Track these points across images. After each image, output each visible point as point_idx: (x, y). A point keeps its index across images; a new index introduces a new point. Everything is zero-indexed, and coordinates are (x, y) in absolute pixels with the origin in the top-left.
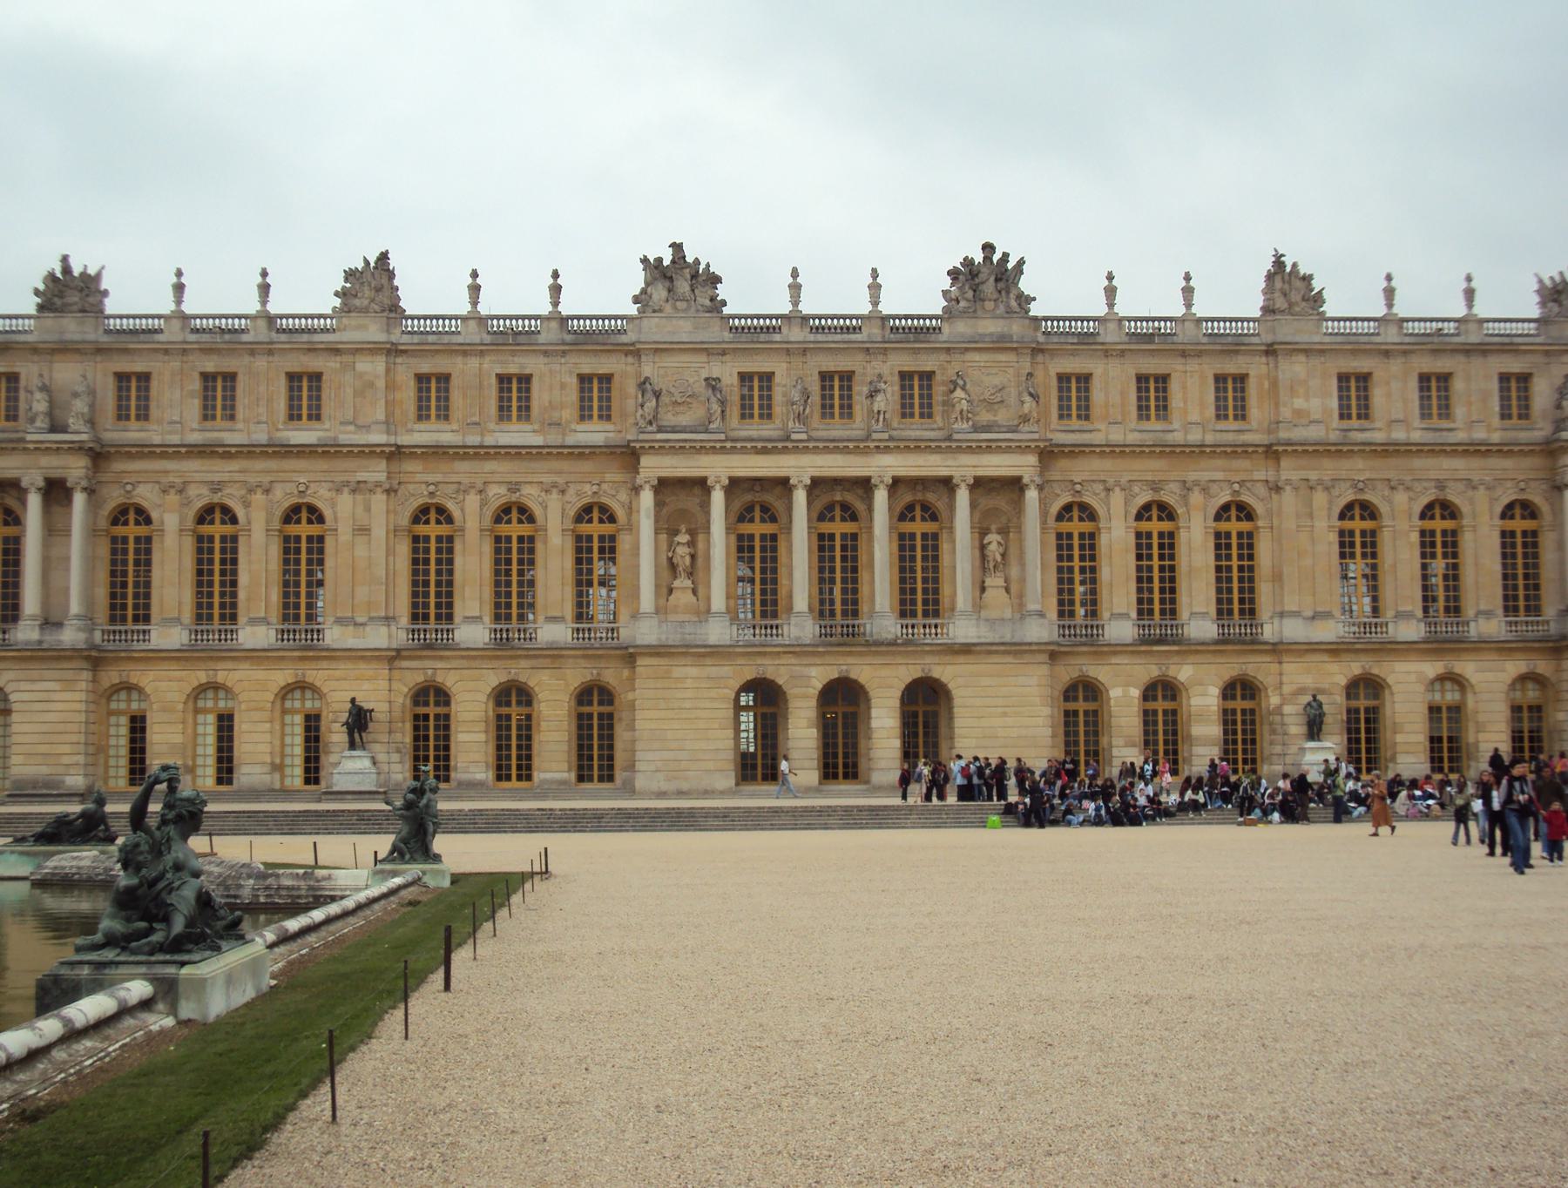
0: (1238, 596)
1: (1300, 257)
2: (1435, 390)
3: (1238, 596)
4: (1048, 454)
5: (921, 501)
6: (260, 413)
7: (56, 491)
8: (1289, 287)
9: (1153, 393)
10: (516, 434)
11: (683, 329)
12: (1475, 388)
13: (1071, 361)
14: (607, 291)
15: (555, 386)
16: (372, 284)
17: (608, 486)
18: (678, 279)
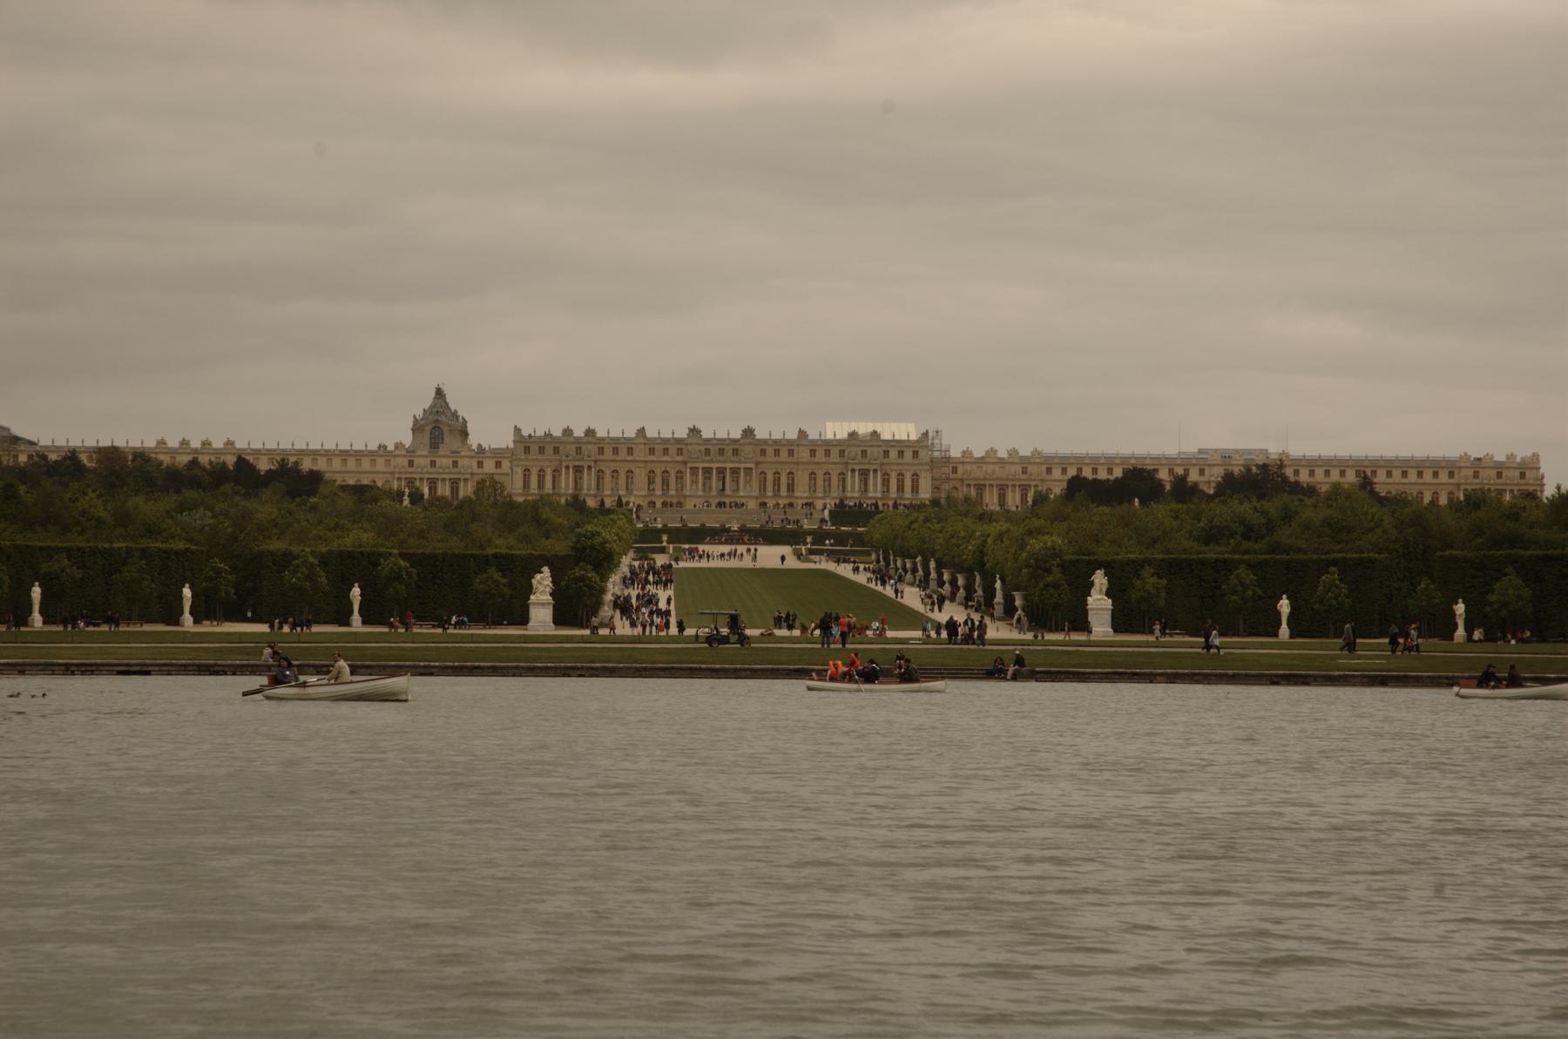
0: (791, 488)
1: (804, 428)
2: (828, 453)
3: (791, 488)
4: (757, 463)
5: (735, 471)
6: (623, 455)
7: (589, 467)
8: (802, 434)
9: (777, 452)
10: (666, 458)
11: (695, 441)
12: (835, 452)
13: (763, 447)
14: (682, 433)
15: (673, 450)
16: (642, 431)
17: (681, 468)
18: (694, 431)
